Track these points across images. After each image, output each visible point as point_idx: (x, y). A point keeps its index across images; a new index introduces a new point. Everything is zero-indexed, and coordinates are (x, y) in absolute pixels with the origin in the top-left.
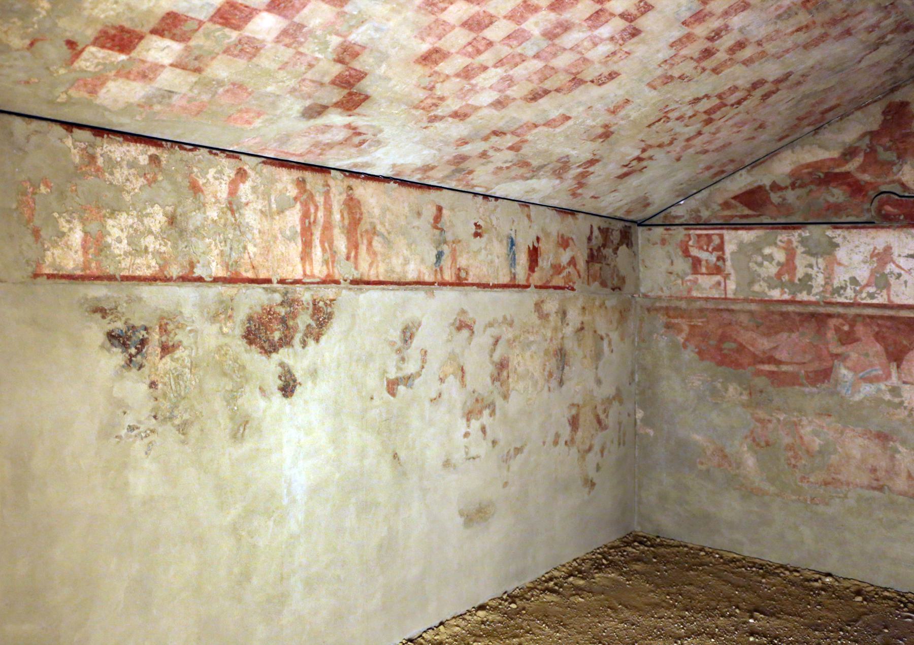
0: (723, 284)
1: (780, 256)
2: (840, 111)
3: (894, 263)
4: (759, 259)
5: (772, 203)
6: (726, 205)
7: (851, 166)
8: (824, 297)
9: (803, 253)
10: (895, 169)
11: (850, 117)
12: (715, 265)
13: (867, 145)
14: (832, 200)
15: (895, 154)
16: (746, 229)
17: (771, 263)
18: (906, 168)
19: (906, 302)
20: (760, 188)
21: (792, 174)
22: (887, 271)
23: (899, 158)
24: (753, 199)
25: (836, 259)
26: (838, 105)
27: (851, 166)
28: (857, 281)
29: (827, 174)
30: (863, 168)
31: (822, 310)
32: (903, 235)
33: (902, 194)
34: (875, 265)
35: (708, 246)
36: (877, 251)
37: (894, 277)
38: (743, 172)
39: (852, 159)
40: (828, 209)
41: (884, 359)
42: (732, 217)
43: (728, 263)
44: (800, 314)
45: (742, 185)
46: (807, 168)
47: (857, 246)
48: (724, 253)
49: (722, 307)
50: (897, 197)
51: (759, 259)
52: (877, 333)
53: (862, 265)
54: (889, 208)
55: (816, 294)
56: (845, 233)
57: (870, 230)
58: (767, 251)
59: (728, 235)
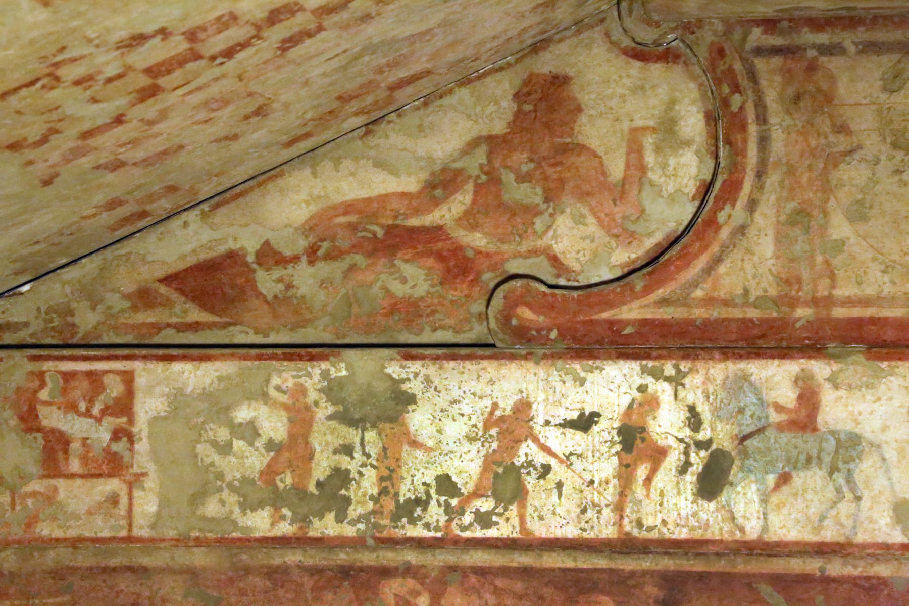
0: (124, 501)
1: (274, 426)
2: (426, 86)
3: (536, 440)
4: (223, 434)
5: (259, 295)
6: (144, 298)
7: (447, 213)
8: (376, 526)
9: (330, 418)
10: (539, 224)
11: (446, 101)
12: (107, 451)
13: (481, 166)
14: (399, 289)
15: (539, 191)
16: (192, 359)
17: (251, 444)
18: (563, 223)
19: (559, 533)
20: (233, 257)
21: (309, 228)
22: (519, 460)
23: (547, 200)
24: (214, 283)
25: (407, 433)
26: (429, 72)
27: (447, 213)
28: (454, 485)
29: (390, 230)
30: (469, 219)
31: (367, 558)
32: (555, 377)
33: (552, 281)
34: (495, 445)
35: (91, 402)
36: (498, 413)
38: (192, 216)
39: (446, 198)
40: (393, 310)
42: (158, 328)
43: (142, 447)
44: (315, 571)
45: (188, 249)
46: (345, 213)
47: (455, 402)
48: (131, 422)
49: (114, 562)
50: (543, 288)
51: (223, 434)
53: (467, 446)
54: (526, 313)
55: (358, 520)
56: (431, 369)
57: (485, 363)
58: (243, 414)
59: (147, 373)
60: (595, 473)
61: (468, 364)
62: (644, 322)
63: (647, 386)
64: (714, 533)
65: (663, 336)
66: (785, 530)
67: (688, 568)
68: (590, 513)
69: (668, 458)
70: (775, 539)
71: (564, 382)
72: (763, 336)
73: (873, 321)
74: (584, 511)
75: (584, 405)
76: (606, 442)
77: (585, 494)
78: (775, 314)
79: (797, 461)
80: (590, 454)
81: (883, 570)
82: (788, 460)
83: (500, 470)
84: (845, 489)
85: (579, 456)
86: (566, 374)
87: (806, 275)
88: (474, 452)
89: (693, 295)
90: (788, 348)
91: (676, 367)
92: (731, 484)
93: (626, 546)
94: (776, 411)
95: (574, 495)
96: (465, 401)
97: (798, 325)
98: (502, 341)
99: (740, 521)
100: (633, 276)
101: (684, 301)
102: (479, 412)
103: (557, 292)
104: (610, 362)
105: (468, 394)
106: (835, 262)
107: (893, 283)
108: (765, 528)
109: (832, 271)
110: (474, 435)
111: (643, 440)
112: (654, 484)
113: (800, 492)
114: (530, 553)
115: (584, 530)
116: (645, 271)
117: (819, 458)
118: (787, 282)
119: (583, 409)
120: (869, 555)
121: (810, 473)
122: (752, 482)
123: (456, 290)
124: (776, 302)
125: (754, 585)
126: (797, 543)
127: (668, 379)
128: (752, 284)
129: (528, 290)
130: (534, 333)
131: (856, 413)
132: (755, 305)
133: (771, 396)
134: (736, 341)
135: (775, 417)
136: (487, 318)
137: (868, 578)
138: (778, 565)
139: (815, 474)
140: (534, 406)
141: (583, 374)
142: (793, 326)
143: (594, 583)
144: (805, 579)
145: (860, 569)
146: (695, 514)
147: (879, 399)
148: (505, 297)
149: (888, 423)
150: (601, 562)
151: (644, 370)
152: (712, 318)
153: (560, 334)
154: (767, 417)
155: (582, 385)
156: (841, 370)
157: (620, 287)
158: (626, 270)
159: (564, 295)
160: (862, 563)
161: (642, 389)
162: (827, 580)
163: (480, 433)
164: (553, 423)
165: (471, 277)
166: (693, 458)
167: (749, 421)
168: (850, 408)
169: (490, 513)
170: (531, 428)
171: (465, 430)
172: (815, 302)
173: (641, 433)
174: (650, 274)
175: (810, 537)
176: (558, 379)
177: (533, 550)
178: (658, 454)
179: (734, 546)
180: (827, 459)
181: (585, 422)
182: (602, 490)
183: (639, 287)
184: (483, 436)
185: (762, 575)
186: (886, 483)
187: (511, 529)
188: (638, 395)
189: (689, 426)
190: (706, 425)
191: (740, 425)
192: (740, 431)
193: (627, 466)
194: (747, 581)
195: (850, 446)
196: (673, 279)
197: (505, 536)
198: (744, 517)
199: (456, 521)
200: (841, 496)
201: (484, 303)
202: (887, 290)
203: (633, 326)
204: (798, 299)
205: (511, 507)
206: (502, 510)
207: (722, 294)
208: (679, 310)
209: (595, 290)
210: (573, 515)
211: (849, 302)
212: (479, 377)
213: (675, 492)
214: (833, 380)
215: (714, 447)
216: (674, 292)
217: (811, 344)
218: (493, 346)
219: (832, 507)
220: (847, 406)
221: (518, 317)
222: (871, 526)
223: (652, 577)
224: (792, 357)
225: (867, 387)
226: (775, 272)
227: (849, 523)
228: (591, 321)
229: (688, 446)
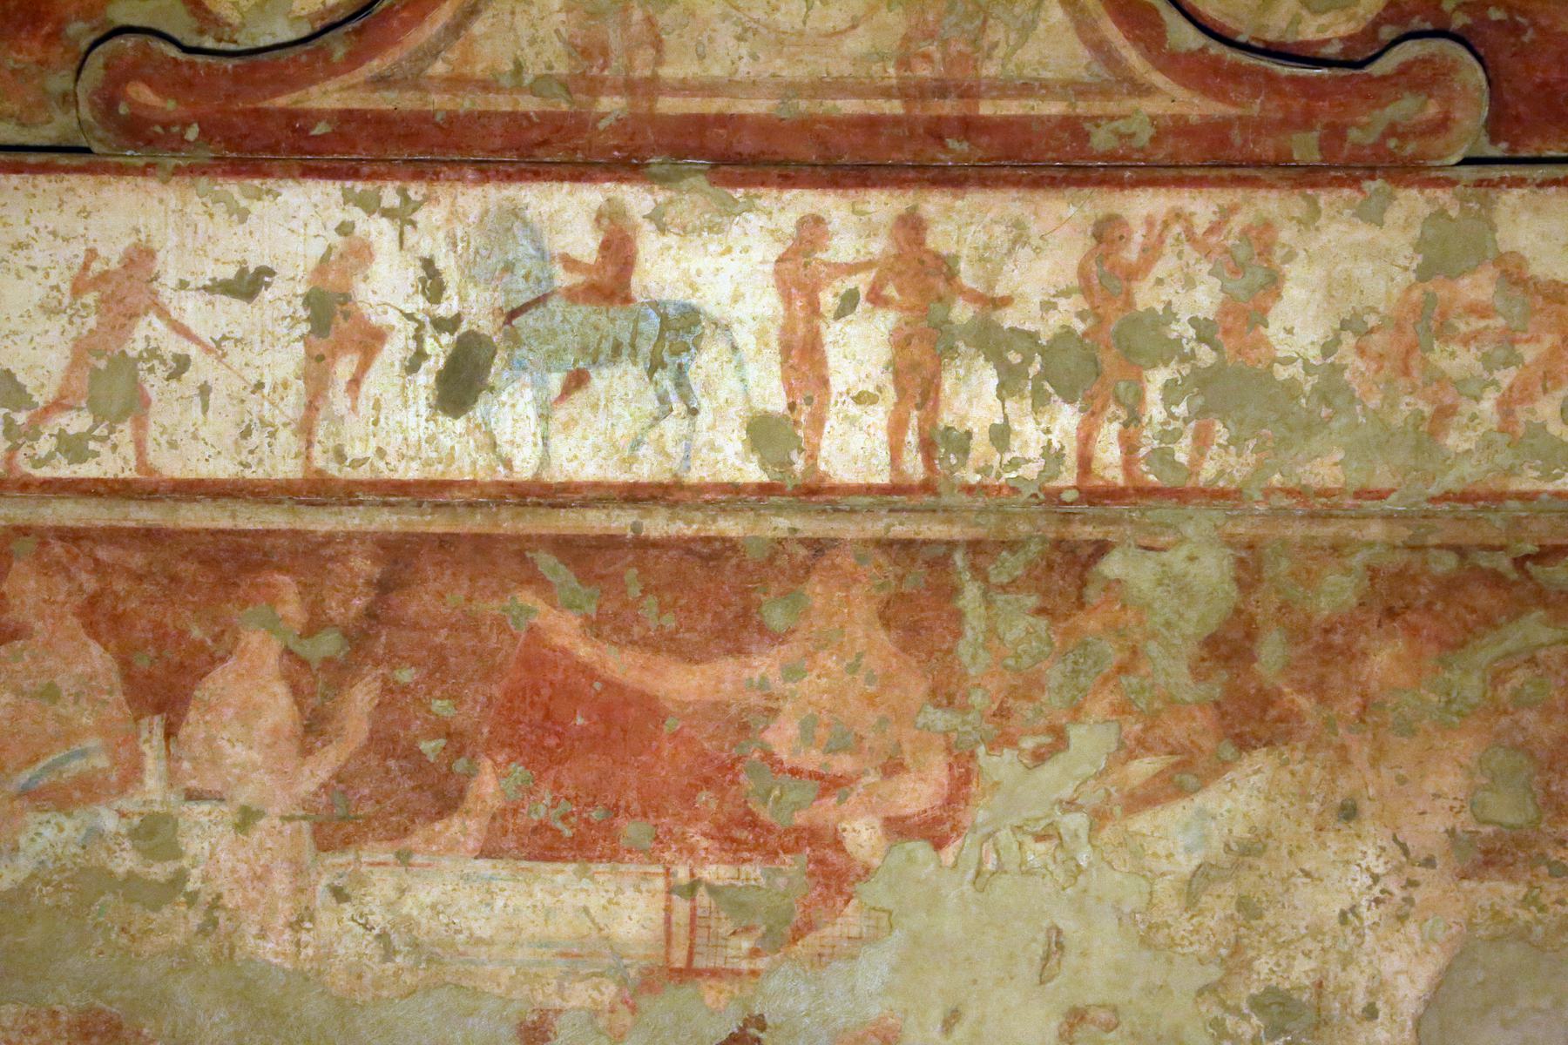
3: (163, 313)
22: (135, 347)
28: (21, 389)
32: (195, 206)
33: (192, 40)
34: (92, 322)
36: (96, 267)
37: (161, 371)
41: (116, 704)
47: (20, 246)
52: (93, 601)
53: (42, 322)
54: (142, 94)
57: (73, 180)
60: (266, 370)
61: (41, 179)
62: (347, 116)
63: (353, 225)
64: (462, 469)
65: (380, 140)
66: (575, 464)
67: (420, 529)
68: (255, 439)
69: (387, 347)
70: (560, 478)
71: (211, 216)
72: (545, 143)
73: (722, 120)
74: (246, 434)
75: (248, 256)
76: (284, 318)
77: (249, 405)
78: (564, 107)
79: (597, 352)
80: (256, 338)
81: (730, 526)
82: (584, 349)
83: (102, 364)
84: (673, 397)
85: (237, 341)
86: (214, 203)
87: (615, 40)
88: (55, 333)
89: (430, 71)
90: (586, 164)
91: (403, 193)
92: (492, 389)
93: (317, 491)
94: (565, 267)
95: (230, 408)
96: (37, 246)
97: (602, 125)
98: (100, 140)
99: (505, 449)
100: (327, 36)
101: (415, 81)
102: (63, 264)
103: (199, 59)
104: (290, 183)
105: (44, 233)
106: (663, 20)
107: (754, 57)
108: (545, 461)
109: (657, 36)
110: (55, 303)
111: (346, 315)
112: (364, 388)
113: (602, 403)
114: (158, 505)
115: (247, 466)
116: (349, 27)
117: (633, 346)
118: (586, 53)
119: (245, 262)
120: (707, 502)
121: (618, 372)
122: (524, 385)
123: (20, 51)
124: (567, 86)
125: (528, 555)
126: (596, 485)
127: (387, 213)
128: (528, 54)
129: (147, 53)
130: (158, 129)
131: (693, 272)
132: (533, 90)
133: (559, 244)
134: (502, 150)
135: (563, 278)
136: (77, 102)
137: (708, 540)
138: (567, 522)
139: (626, 373)
140: (160, 256)
141: (243, 203)
142: (595, 127)
143: (265, 554)
144: (609, 543)
145: (695, 527)
146: (431, 440)
147: (729, 250)
148: (106, 66)
149: (742, 289)
150: (276, 519)
151: (348, 198)
152: (461, 111)
153: (202, 132)
154: (551, 278)
155: (243, 220)
156: (671, 202)
157: (308, 53)
158: (318, 25)
159: (209, 66)
160: (699, 516)
161: (345, 229)
162: (643, 544)
163: (66, 301)
164: (192, 285)
165: (47, 29)
166: (429, 345)
167: (522, 285)
168: (684, 265)
169: (81, 438)
170: (155, 293)
171: (38, 294)
172: (629, 87)
173: (343, 304)
174: (358, 32)
175: (616, 475)
176: (201, 209)
177: (160, 499)
178: (371, 340)
179: (493, 491)
180: (645, 348)
181: (248, 285)
182: (277, 398)
183: (339, 53)
184: (70, 306)
185: (541, 538)
186: (738, 386)
187: (120, 463)
188: (337, 240)
189: (423, 292)
190: (451, 291)
191: (507, 292)
192: (507, 302)
193: (321, 358)
194: (516, 547)
195: (683, 328)
196: (396, 43)
197: (110, 476)
198: (512, 443)
199: (24, 449)
200: (667, 407)
201: (70, 76)
202: (745, 68)
203: (329, 122)
204: (603, 81)
205: (120, 427)
206: (106, 432)
207: (479, 69)
208: (409, 95)
209: (260, 57)
210: (229, 442)
211: (684, 88)
212: (61, 204)
213: (399, 402)
214: (658, 220)
215: (464, 328)
216: (398, 64)
217: (623, 159)
218: (87, 151)
219: (651, 426)
220: (678, 261)
221: (132, 103)
222: (713, 455)
223: (363, 542)
224: (591, 179)
225: (710, 229)
226: (565, 35)
227: (677, 451)
228: (257, 110)
229: (421, 326)
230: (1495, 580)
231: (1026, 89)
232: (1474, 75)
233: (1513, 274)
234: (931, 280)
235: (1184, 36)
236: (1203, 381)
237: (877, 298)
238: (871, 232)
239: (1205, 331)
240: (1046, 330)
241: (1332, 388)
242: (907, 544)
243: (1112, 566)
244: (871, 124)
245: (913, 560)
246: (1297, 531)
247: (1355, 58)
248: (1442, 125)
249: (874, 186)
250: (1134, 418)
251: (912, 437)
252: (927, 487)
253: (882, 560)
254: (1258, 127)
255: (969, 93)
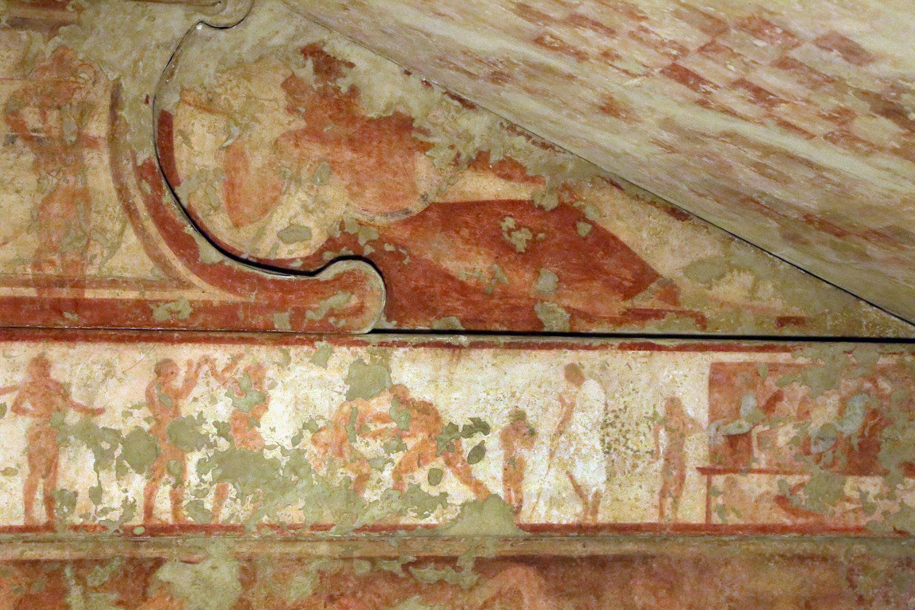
230: (392, 577)
231: (114, 283)
232: (378, 283)
233: (401, 398)
234: (53, 399)
235: (211, 255)
236: (221, 459)
237: (18, 409)
238: (15, 369)
239: (223, 430)
240: (126, 428)
241: (298, 464)
242: (35, 563)
243: (165, 574)
244: (16, 303)
245: (38, 573)
246: (277, 550)
247: (309, 270)
248: (360, 310)
249: (17, 340)
250: (179, 482)
251: (39, 496)
252: (49, 527)
253: (17, 573)
254: (255, 308)
255: (78, 285)
